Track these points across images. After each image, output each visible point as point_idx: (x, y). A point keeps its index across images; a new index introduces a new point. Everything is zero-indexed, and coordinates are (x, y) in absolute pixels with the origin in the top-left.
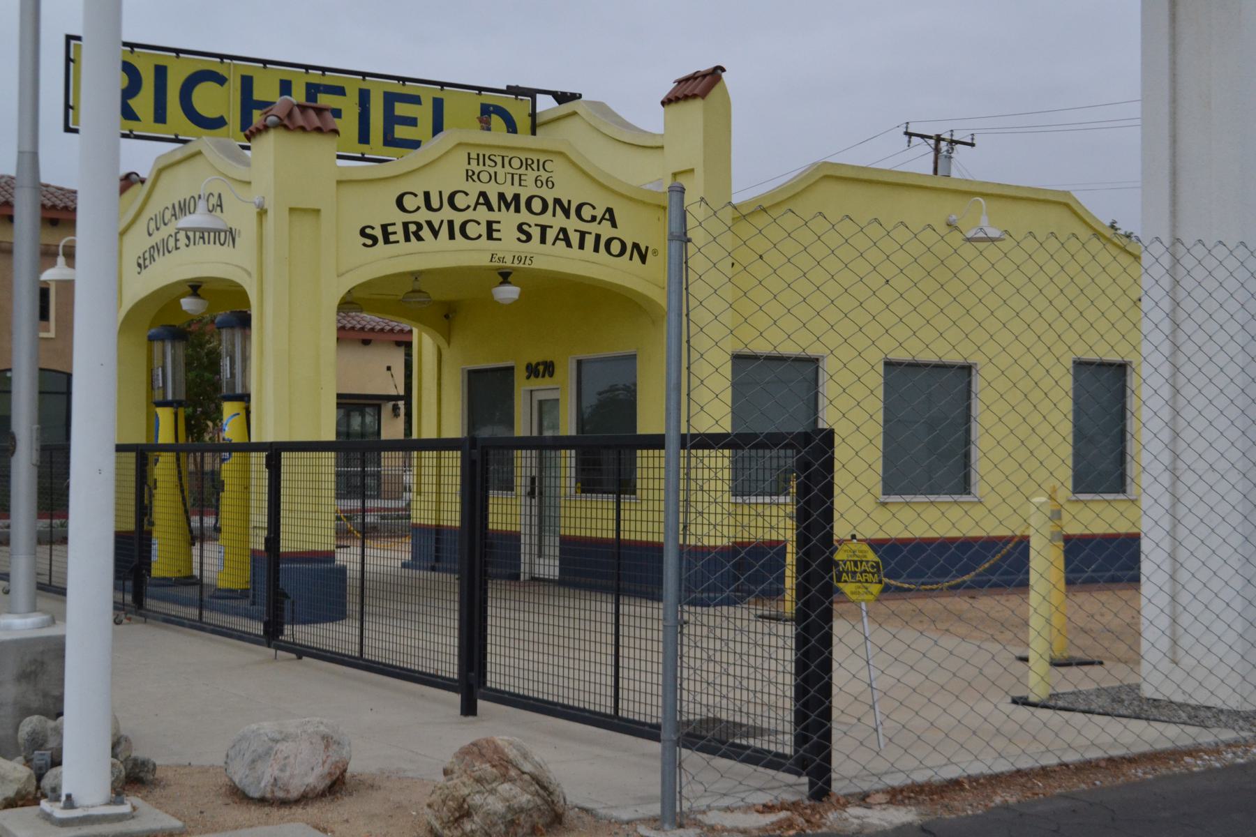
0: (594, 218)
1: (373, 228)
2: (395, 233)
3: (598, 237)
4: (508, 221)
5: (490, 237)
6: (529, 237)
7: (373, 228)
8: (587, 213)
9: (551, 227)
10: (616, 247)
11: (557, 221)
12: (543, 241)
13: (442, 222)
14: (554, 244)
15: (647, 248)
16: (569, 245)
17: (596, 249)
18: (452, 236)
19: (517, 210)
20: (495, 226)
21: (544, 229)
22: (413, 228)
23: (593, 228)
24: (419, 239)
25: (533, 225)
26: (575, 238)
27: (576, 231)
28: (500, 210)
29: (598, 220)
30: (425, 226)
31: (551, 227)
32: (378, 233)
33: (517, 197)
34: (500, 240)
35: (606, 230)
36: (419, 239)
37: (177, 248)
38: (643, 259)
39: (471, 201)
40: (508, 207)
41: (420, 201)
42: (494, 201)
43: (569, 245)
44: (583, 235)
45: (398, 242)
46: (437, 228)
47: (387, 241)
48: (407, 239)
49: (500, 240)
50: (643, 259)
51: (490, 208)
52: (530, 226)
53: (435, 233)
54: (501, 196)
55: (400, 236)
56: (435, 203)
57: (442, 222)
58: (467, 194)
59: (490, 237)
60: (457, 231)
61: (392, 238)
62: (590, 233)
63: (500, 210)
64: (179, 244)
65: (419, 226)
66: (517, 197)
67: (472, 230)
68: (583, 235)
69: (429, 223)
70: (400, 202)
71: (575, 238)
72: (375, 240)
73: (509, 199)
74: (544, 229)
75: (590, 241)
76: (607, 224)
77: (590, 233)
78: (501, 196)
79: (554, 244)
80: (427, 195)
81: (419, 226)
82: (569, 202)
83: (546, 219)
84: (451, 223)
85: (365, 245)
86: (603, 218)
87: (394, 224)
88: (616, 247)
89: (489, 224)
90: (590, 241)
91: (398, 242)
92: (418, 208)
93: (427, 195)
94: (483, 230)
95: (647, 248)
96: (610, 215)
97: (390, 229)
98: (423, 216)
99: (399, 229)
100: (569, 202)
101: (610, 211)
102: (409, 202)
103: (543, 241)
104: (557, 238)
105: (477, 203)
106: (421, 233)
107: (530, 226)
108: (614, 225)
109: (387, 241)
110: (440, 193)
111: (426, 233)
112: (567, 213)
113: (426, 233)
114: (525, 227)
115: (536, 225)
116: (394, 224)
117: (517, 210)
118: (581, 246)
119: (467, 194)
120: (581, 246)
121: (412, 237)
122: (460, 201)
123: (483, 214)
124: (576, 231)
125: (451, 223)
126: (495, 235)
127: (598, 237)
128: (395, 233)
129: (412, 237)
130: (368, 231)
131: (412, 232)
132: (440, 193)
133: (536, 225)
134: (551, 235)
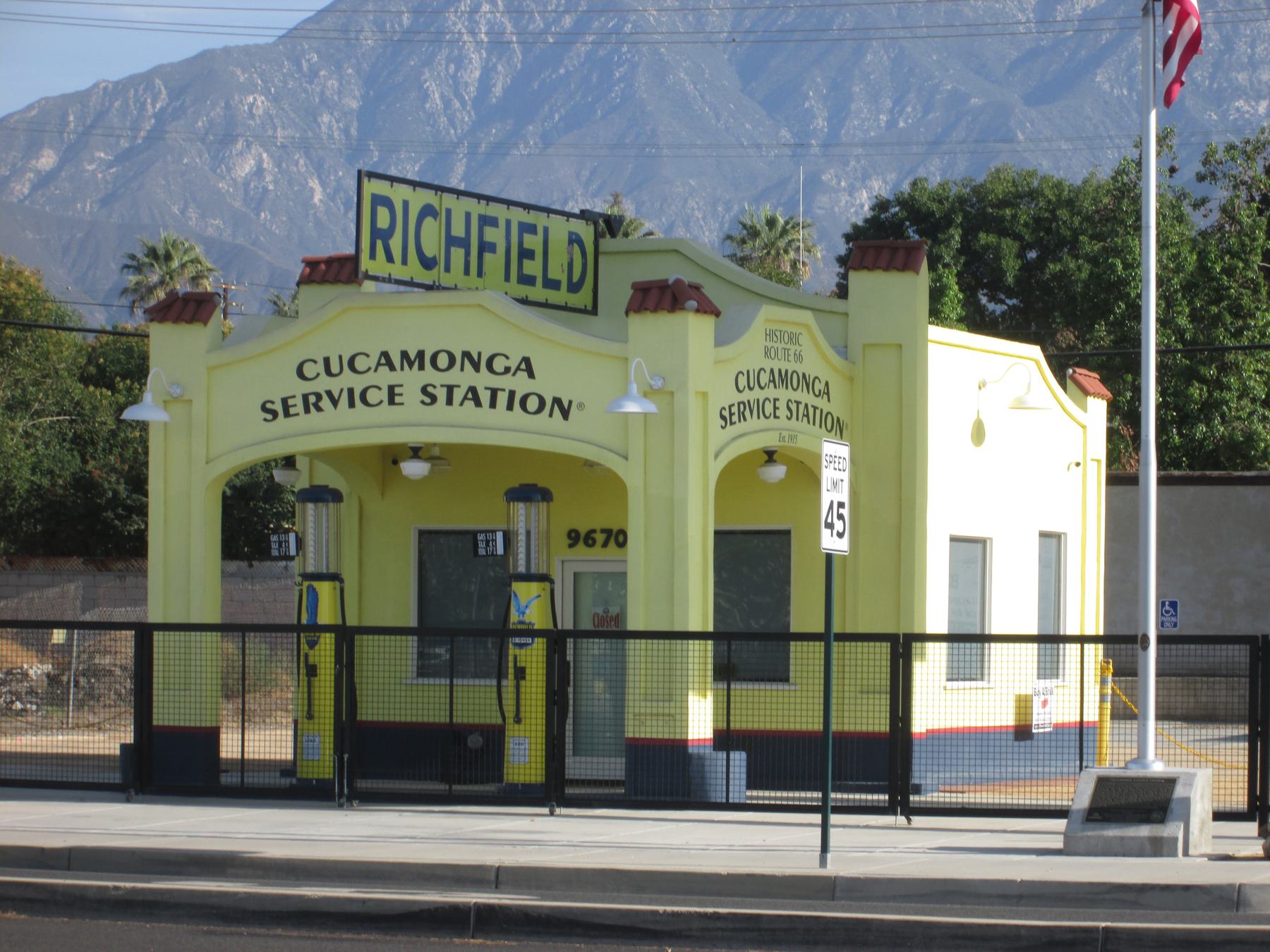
0: (507, 370)
1: (273, 402)
2: (295, 405)
3: (512, 394)
4: (411, 380)
5: (391, 402)
6: (434, 399)
7: (273, 402)
8: (499, 365)
9: (459, 386)
10: (533, 404)
11: (464, 378)
12: (449, 401)
13: (342, 390)
14: (461, 404)
15: (570, 402)
16: (478, 403)
17: (510, 407)
18: (352, 404)
19: (421, 367)
20: (397, 390)
21: (450, 389)
22: (312, 399)
23: (506, 382)
24: (319, 409)
25: (438, 386)
26: (485, 397)
27: (486, 388)
28: (402, 369)
29: (513, 370)
30: (325, 397)
31: (459, 386)
32: (278, 407)
33: (421, 354)
34: (402, 404)
35: (521, 384)
36: (319, 409)
37: (776, 417)
38: (565, 414)
39: (372, 362)
40: (411, 365)
41: (320, 367)
42: (396, 360)
43: (478, 403)
44: (494, 393)
45: (297, 414)
46: (336, 397)
47: (287, 414)
48: (307, 411)
49: (402, 404)
50: (565, 414)
51: (392, 368)
52: (434, 387)
53: (335, 402)
54: (404, 355)
55: (300, 408)
56: (335, 368)
57: (342, 390)
58: (368, 356)
59: (391, 402)
60: (354, 398)
61: (292, 411)
62: (504, 390)
63: (402, 369)
64: (778, 413)
65: (319, 397)
66: (421, 354)
67: (372, 396)
68: (494, 393)
69: (329, 393)
70: (300, 374)
71: (485, 397)
72: (275, 414)
73: (412, 356)
74: (450, 389)
75: (502, 398)
76: (523, 375)
77: (504, 390)
78: (404, 355)
79: (461, 404)
80: (327, 361)
81: (319, 397)
82: (480, 354)
83: (453, 376)
84: (351, 391)
85: (265, 420)
86: (518, 369)
87: (294, 397)
88: (533, 404)
89: (391, 389)
90: (502, 398)
91: (297, 414)
92: (318, 375)
93: (327, 361)
94: (384, 395)
95: (570, 402)
96: (527, 366)
97: (290, 402)
98: (323, 384)
99: (299, 401)
100: (480, 354)
101: (526, 360)
102: (309, 370)
103: (449, 401)
104: (465, 398)
105: (379, 364)
106: (321, 404)
107: (434, 387)
108: (531, 375)
109: (287, 414)
110: (340, 357)
111: (326, 402)
112: (476, 367)
113: (326, 402)
114: (430, 389)
115: (442, 386)
116: (294, 397)
117: (421, 367)
118: (493, 404)
119: (368, 356)
120: (493, 404)
121: (312, 408)
122: (360, 363)
123: (385, 377)
124: (486, 388)
125: (351, 391)
126: (397, 399)
127: (512, 394)
128: (295, 405)
129: (312, 408)
130: (269, 406)
131: (311, 403)
132: (340, 357)
133: (442, 386)
134: (458, 395)
